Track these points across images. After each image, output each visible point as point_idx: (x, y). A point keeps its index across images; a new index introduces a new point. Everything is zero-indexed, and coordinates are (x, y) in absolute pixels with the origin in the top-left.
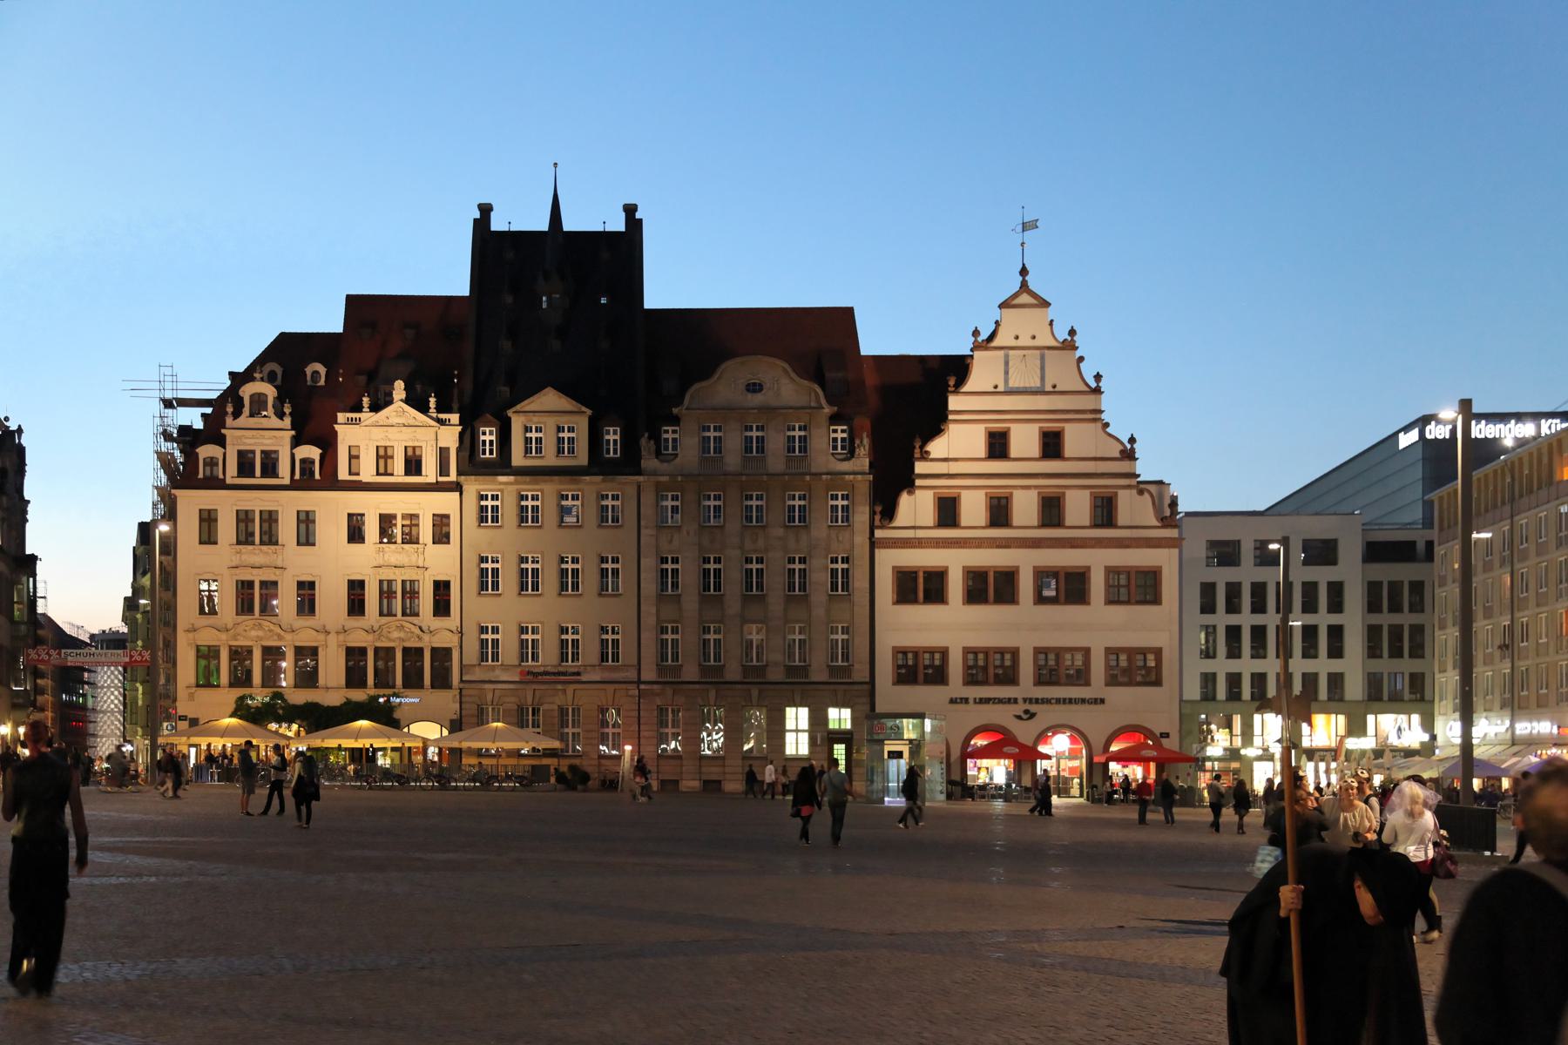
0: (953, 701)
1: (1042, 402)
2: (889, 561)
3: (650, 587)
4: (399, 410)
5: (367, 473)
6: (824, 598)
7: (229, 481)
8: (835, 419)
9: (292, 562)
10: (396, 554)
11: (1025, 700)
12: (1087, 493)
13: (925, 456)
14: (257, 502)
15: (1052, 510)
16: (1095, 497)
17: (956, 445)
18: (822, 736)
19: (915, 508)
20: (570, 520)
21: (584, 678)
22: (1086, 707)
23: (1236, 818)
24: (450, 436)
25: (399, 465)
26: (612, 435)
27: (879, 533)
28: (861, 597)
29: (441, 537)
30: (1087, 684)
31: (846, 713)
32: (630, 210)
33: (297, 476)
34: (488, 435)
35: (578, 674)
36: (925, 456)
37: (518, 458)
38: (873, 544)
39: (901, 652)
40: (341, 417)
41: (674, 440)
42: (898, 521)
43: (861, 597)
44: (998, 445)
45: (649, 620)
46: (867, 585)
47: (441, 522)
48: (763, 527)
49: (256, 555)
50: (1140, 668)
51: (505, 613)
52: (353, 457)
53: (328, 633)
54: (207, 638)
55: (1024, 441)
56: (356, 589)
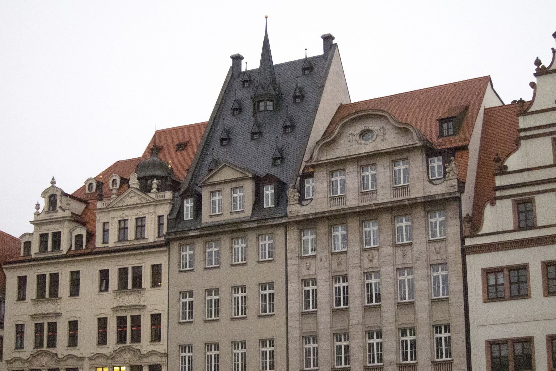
3: (295, 306)
4: (133, 198)
5: (113, 240)
6: (426, 303)
7: (33, 256)
8: (430, 151)
9: (67, 307)
10: (129, 299)
13: (503, 171)
14: (47, 271)
19: (498, 217)
24: (164, 210)
25: (131, 234)
26: (269, 191)
27: (468, 242)
28: (457, 300)
29: (156, 282)
32: (328, 39)
33: (73, 248)
34: (189, 204)
36: (503, 171)
37: (205, 219)
38: (465, 251)
40: (99, 205)
41: (313, 187)
42: (485, 229)
45: (295, 334)
46: (462, 288)
47: (156, 270)
48: (377, 249)
49: (47, 307)
52: (105, 231)
56: (103, 323)
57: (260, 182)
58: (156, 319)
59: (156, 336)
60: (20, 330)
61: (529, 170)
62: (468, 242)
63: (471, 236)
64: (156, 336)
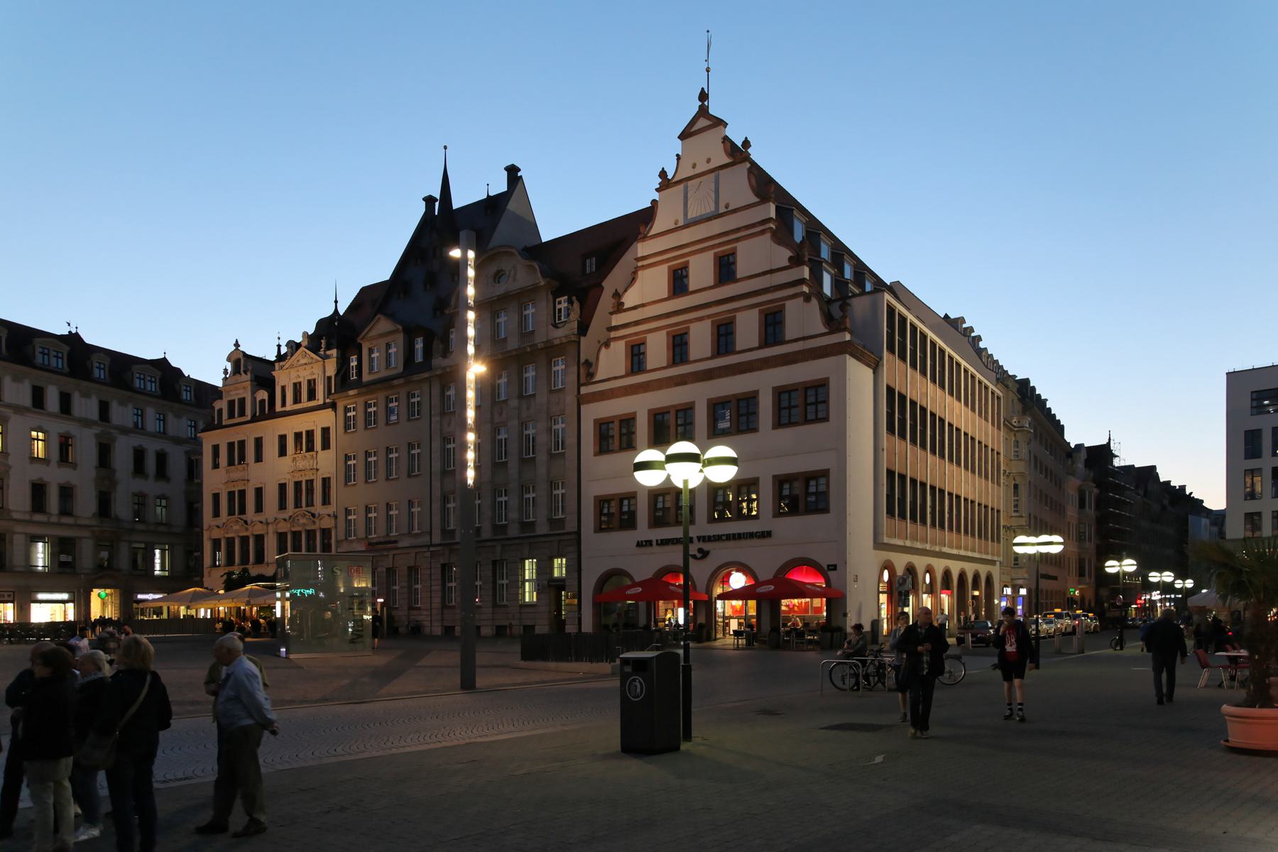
0: (639, 544)
1: (716, 227)
2: (594, 412)
10: (304, 461)
11: (699, 538)
12: (755, 312)
14: (235, 435)
15: (724, 336)
16: (761, 312)
17: (646, 289)
18: (549, 586)
20: (394, 418)
21: (400, 545)
22: (755, 542)
23: (256, 816)
24: (331, 368)
27: (584, 390)
29: (326, 445)
30: (599, 529)
31: (557, 562)
35: (396, 542)
39: (602, 502)
43: (571, 453)
44: (679, 282)
49: (237, 473)
50: (813, 494)
51: (352, 498)
53: (268, 524)
54: (217, 534)
55: (701, 270)
57: (410, 333)
58: (326, 482)
59: (326, 501)
60: (216, 497)
61: (643, 305)
62: (584, 390)
63: (588, 384)
64: (326, 501)
